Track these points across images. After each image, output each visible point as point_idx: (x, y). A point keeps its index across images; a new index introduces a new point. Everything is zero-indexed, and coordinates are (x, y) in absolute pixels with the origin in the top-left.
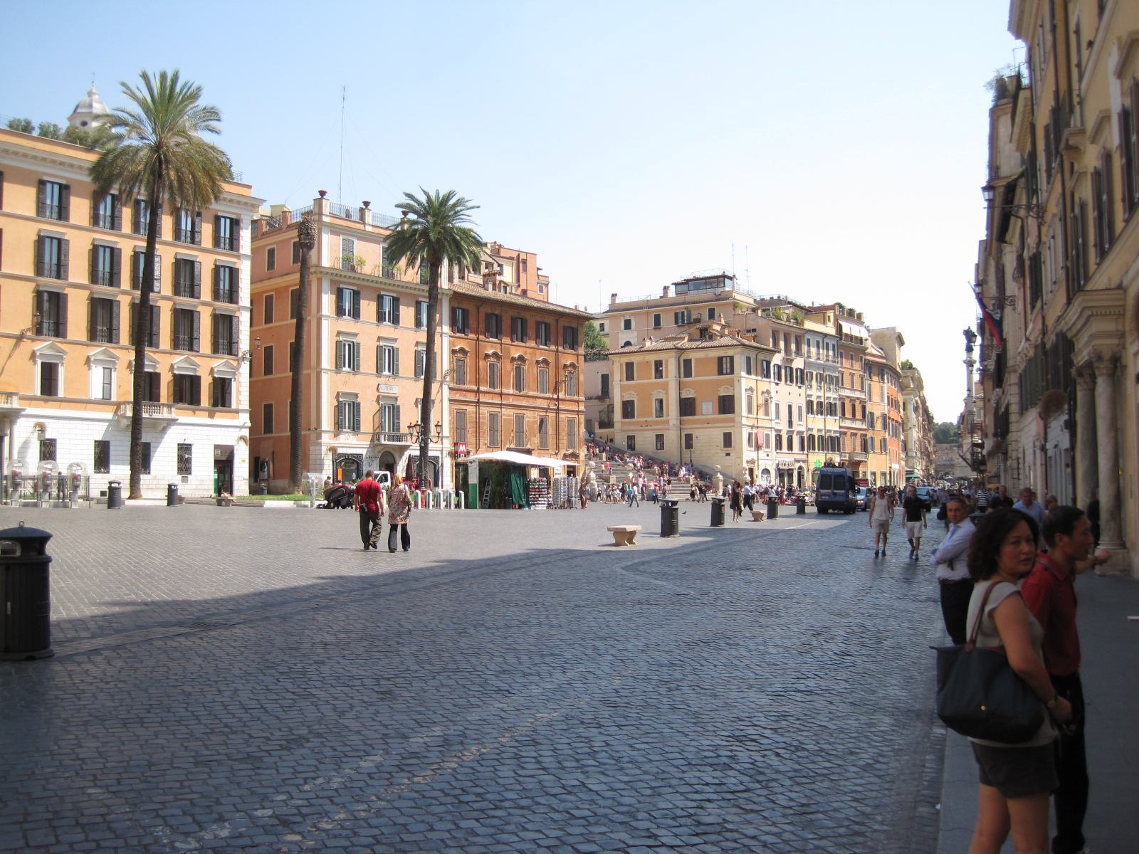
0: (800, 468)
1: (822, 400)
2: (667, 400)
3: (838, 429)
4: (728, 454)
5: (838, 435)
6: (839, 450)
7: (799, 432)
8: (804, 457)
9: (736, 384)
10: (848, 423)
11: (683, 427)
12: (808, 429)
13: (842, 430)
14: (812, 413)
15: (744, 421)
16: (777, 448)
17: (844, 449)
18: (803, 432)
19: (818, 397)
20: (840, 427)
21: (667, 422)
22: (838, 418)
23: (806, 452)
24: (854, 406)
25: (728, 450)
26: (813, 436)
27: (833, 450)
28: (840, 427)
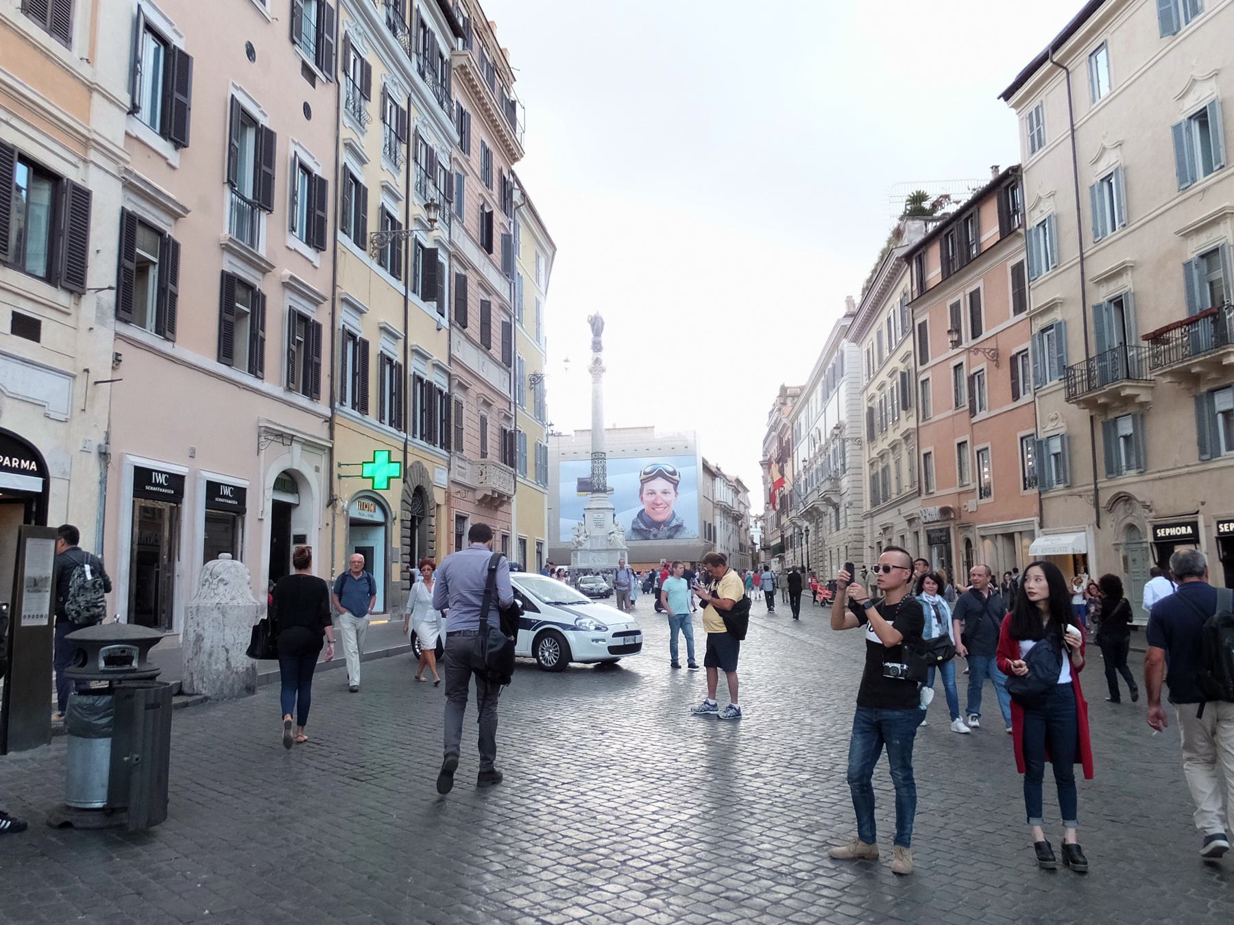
0: (289, 481)
1: (399, 216)
3: (444, 361)
5: (440, 382)
6: (446, 445)
7: (291, 285)
8: (317, 430)
10: (470, 356)
12: (338, 300)
13: (455, 370)
14: (360, 241)
17: (460, 448)
18: (315, 300)
19: (386, 188)
20: (451, 358)
22: (445, 322)
23: (323, 407)
24: (485, 307)
26: (362, 347)
27: (429, 436)
28: (451, 358)
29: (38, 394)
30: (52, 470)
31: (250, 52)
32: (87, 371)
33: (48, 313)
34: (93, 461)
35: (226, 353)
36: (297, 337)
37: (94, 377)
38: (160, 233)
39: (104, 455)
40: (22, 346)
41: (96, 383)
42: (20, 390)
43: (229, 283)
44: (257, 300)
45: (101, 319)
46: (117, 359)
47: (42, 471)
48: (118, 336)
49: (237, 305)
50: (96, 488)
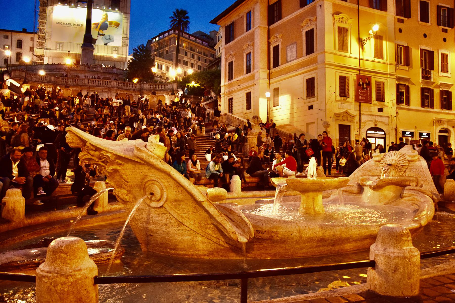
2: (254, 52)
4: (311, 107)
9: (318, 9)
11: (272, 81)
15: (329, 59)
16: (399, 101)
25: (312, 101)
30: (386, 134)
31: (425, 36)
34: (394, 131)
35: (423, 105)
36: (444, 96)
37: (393, 116)
38: (405, 85)
39: (396, 130)
40: (380, 113)
42: (380, 121)
43: (423, 90)
44: (431, 91)
45: (393, 106)
46: (397, 112)
47: (385, 134)
48: (397, 108)
49: (425, 94)
50: (395, 136)
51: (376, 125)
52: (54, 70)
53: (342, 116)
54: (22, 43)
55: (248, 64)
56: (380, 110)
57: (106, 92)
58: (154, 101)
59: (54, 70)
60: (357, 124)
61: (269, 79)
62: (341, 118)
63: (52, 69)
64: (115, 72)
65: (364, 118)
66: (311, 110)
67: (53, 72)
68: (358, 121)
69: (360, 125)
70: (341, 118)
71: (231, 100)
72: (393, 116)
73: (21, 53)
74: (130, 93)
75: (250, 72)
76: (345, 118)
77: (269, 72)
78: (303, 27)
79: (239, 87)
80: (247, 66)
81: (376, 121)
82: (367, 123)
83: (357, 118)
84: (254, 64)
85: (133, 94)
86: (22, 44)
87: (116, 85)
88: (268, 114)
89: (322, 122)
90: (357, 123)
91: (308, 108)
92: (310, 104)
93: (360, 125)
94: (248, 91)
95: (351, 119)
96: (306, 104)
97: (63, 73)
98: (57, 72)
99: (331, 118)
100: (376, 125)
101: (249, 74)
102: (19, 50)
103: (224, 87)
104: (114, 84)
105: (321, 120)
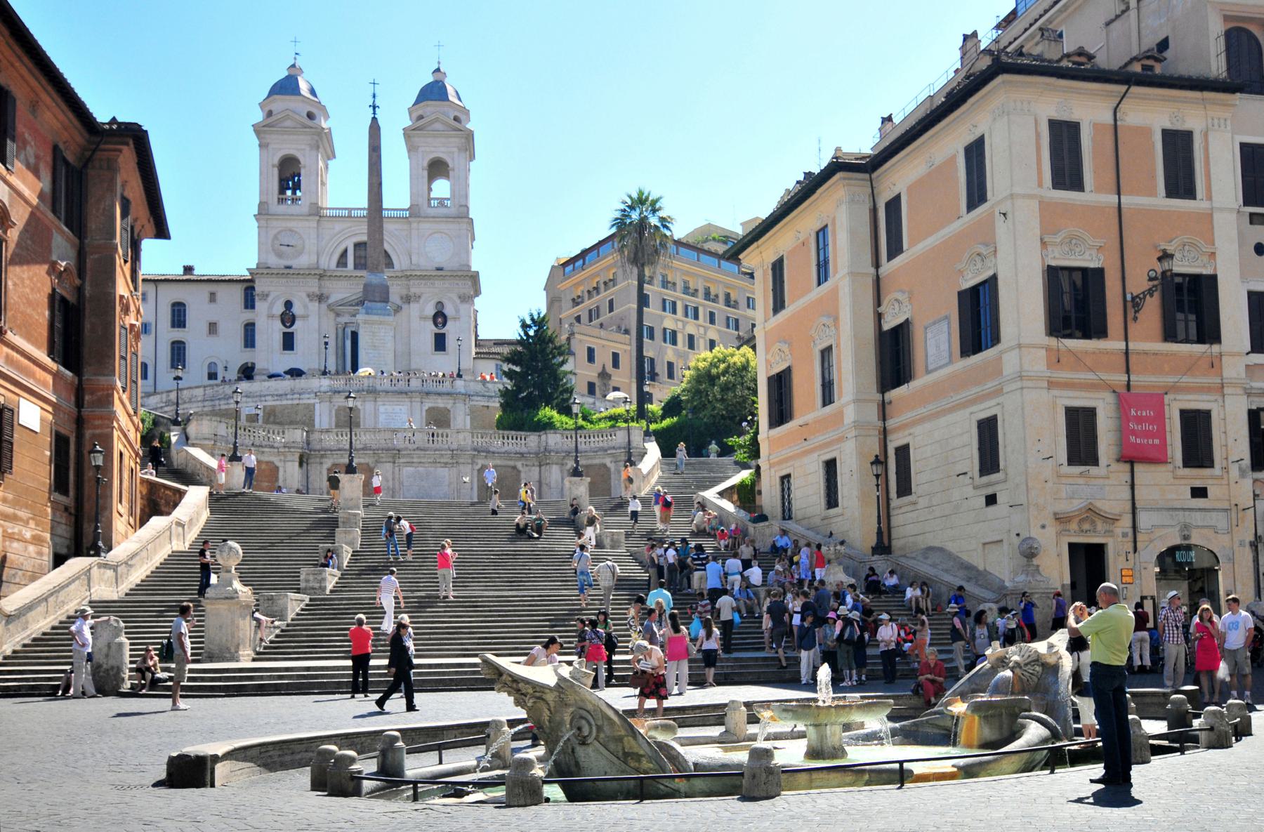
11: (891, 423)
21: (840, 415)
29: (1212, 523)
32: (1236, 505)
33: (1210, 482)
37: (1240, 507)
40: (1200, 502)
41: (1244, 510)
48: (1255, 481)
51: (1186, 537)
52: (286, 395)
53: (1077, 520)
54: (185, 311)
55: (827, 380)
56: (1199, 492)
57: (446, 463)
58: (579, 494)
59: (286, 395)
60: (1124, 539)
61: (884, 417)
62: (1074, 526)
63: (280, 392)
64: (463, 391)
65: (1144, 520)
66: (992, 508)
67: (285, 402)
68: (1130, 531)
69: (1135, 542)
70: (1074, 526)
71: (786, 478)
72: (1240, 507)
73: (184, 343)
74: (511, 463)
75: (831, 402)
76: (1086, 526)
77: (883, 400)
78: (965, 273)
79: (806, 443)
80: (823, 385)
81: (1186, 527)
82: (1158, 533)
83: (1126, 522)
84: (840, 379)
85: (519, 465)
86: (185, 316)
87: (470, 443)
88: (879, 523)
89: (1017, 541)
90: (1125, 535)
91: (983, 500)
92: (990, 491)
93: (1135, 542)
94: (828, 457)
95: (1107, 527)
96: (978, 492)
97: (312, 401)
98: (296, 402)
99: (1043, 527)
100: (1186, 537)
101: (828, 408)
102: (178, 334)
103: (767, 442)
104: (465, 440)
105: (1018, 535)
